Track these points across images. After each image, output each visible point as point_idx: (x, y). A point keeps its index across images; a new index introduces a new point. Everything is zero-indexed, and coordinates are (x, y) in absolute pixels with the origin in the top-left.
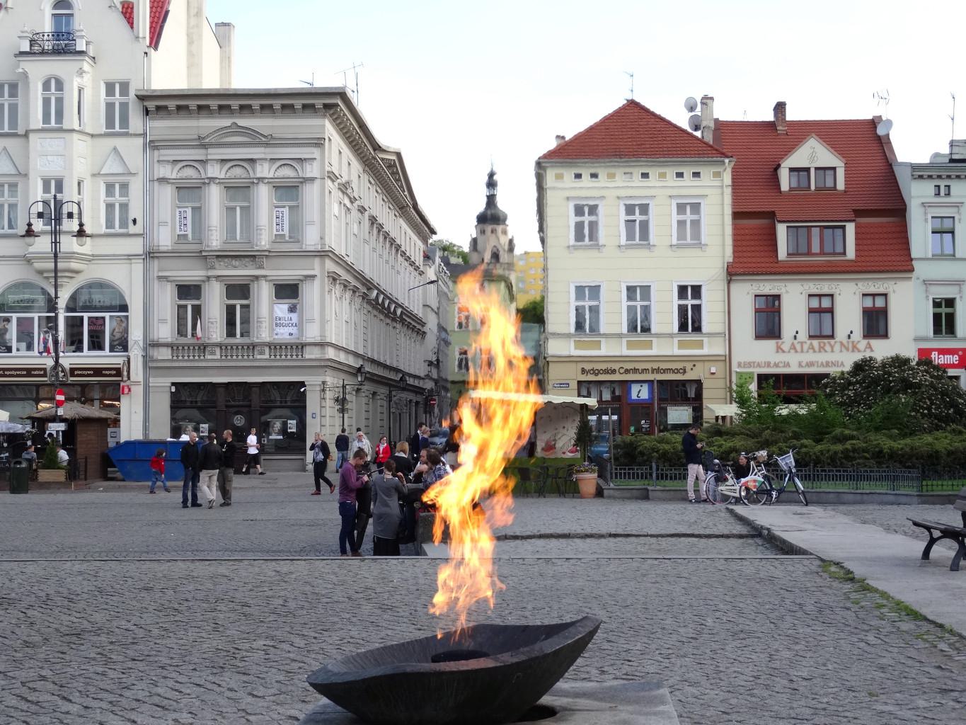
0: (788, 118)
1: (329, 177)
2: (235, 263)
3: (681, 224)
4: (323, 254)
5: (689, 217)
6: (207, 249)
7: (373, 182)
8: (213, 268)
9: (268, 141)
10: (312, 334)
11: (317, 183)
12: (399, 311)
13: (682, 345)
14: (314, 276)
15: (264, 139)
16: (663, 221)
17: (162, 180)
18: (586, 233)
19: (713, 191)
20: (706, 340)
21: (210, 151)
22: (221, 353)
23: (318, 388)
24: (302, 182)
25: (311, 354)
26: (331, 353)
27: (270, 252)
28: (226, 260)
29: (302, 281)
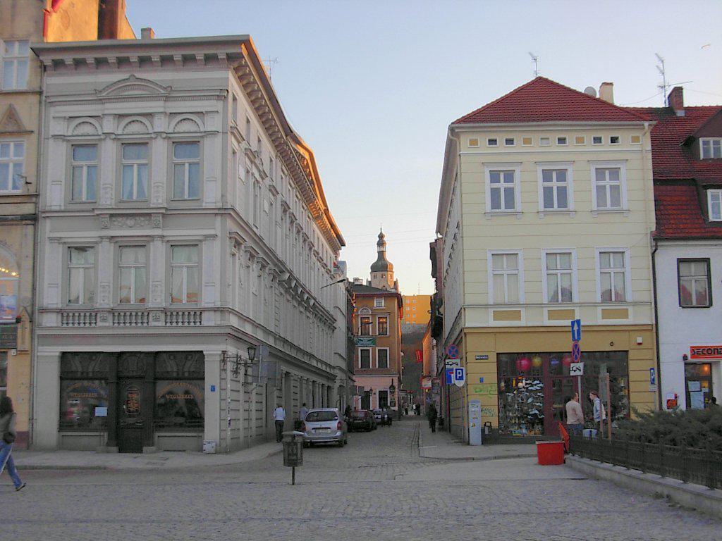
0: (686, 104)
1: (232, 133)
2: (130, 222)
3: (601, 190)
4: (225, 212)
5: (608, 182)
6: (100, 207)
7: (286, 172)
8: (105, 228)
9: (169, 94)
10: (210, 298)
11: (220, 137)
12: (312, 302)
15: (163, 92)
16: (581, 187)
17: (55, 136)
18: (503, 200)
19: (634, 158)
20: (631, 309)
21: (107, 105)
22: (114, 320)
23: (218, 358)
24: (202, 137)
25: (210, 320)
26: (234, 321)
27: (166, 209)
28: (120, 219)
29: (200, 241)
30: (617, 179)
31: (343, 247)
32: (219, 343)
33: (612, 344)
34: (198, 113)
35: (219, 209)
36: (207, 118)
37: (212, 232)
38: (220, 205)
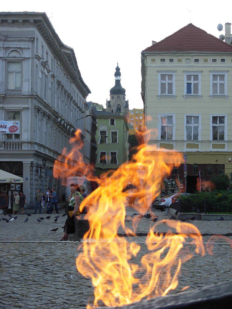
1: (36, 58)
3: (215, 85)
5: (218, 82)
7: (59, 64)
11: (30, 60)
13: (214, 146)
14: (28, 108)
15: (3, 38)
18: (167, 90)
20: (226, 144)
23: (29, 165)
24: (22, 60)
25: (25, 147)
26: (36, 148)
29: (21, 110)
30: (223, 80)
31: (89, 94)
32: (30, 158)
33: (217, 161)
34: (20, 48)
35: (30, 95)
36: (24, 51)
37: (26, 106)
38: (30, 93)
